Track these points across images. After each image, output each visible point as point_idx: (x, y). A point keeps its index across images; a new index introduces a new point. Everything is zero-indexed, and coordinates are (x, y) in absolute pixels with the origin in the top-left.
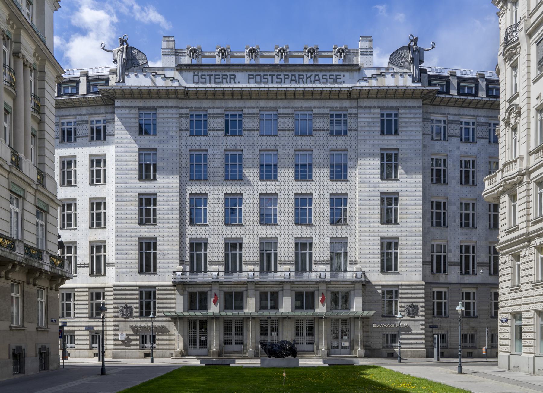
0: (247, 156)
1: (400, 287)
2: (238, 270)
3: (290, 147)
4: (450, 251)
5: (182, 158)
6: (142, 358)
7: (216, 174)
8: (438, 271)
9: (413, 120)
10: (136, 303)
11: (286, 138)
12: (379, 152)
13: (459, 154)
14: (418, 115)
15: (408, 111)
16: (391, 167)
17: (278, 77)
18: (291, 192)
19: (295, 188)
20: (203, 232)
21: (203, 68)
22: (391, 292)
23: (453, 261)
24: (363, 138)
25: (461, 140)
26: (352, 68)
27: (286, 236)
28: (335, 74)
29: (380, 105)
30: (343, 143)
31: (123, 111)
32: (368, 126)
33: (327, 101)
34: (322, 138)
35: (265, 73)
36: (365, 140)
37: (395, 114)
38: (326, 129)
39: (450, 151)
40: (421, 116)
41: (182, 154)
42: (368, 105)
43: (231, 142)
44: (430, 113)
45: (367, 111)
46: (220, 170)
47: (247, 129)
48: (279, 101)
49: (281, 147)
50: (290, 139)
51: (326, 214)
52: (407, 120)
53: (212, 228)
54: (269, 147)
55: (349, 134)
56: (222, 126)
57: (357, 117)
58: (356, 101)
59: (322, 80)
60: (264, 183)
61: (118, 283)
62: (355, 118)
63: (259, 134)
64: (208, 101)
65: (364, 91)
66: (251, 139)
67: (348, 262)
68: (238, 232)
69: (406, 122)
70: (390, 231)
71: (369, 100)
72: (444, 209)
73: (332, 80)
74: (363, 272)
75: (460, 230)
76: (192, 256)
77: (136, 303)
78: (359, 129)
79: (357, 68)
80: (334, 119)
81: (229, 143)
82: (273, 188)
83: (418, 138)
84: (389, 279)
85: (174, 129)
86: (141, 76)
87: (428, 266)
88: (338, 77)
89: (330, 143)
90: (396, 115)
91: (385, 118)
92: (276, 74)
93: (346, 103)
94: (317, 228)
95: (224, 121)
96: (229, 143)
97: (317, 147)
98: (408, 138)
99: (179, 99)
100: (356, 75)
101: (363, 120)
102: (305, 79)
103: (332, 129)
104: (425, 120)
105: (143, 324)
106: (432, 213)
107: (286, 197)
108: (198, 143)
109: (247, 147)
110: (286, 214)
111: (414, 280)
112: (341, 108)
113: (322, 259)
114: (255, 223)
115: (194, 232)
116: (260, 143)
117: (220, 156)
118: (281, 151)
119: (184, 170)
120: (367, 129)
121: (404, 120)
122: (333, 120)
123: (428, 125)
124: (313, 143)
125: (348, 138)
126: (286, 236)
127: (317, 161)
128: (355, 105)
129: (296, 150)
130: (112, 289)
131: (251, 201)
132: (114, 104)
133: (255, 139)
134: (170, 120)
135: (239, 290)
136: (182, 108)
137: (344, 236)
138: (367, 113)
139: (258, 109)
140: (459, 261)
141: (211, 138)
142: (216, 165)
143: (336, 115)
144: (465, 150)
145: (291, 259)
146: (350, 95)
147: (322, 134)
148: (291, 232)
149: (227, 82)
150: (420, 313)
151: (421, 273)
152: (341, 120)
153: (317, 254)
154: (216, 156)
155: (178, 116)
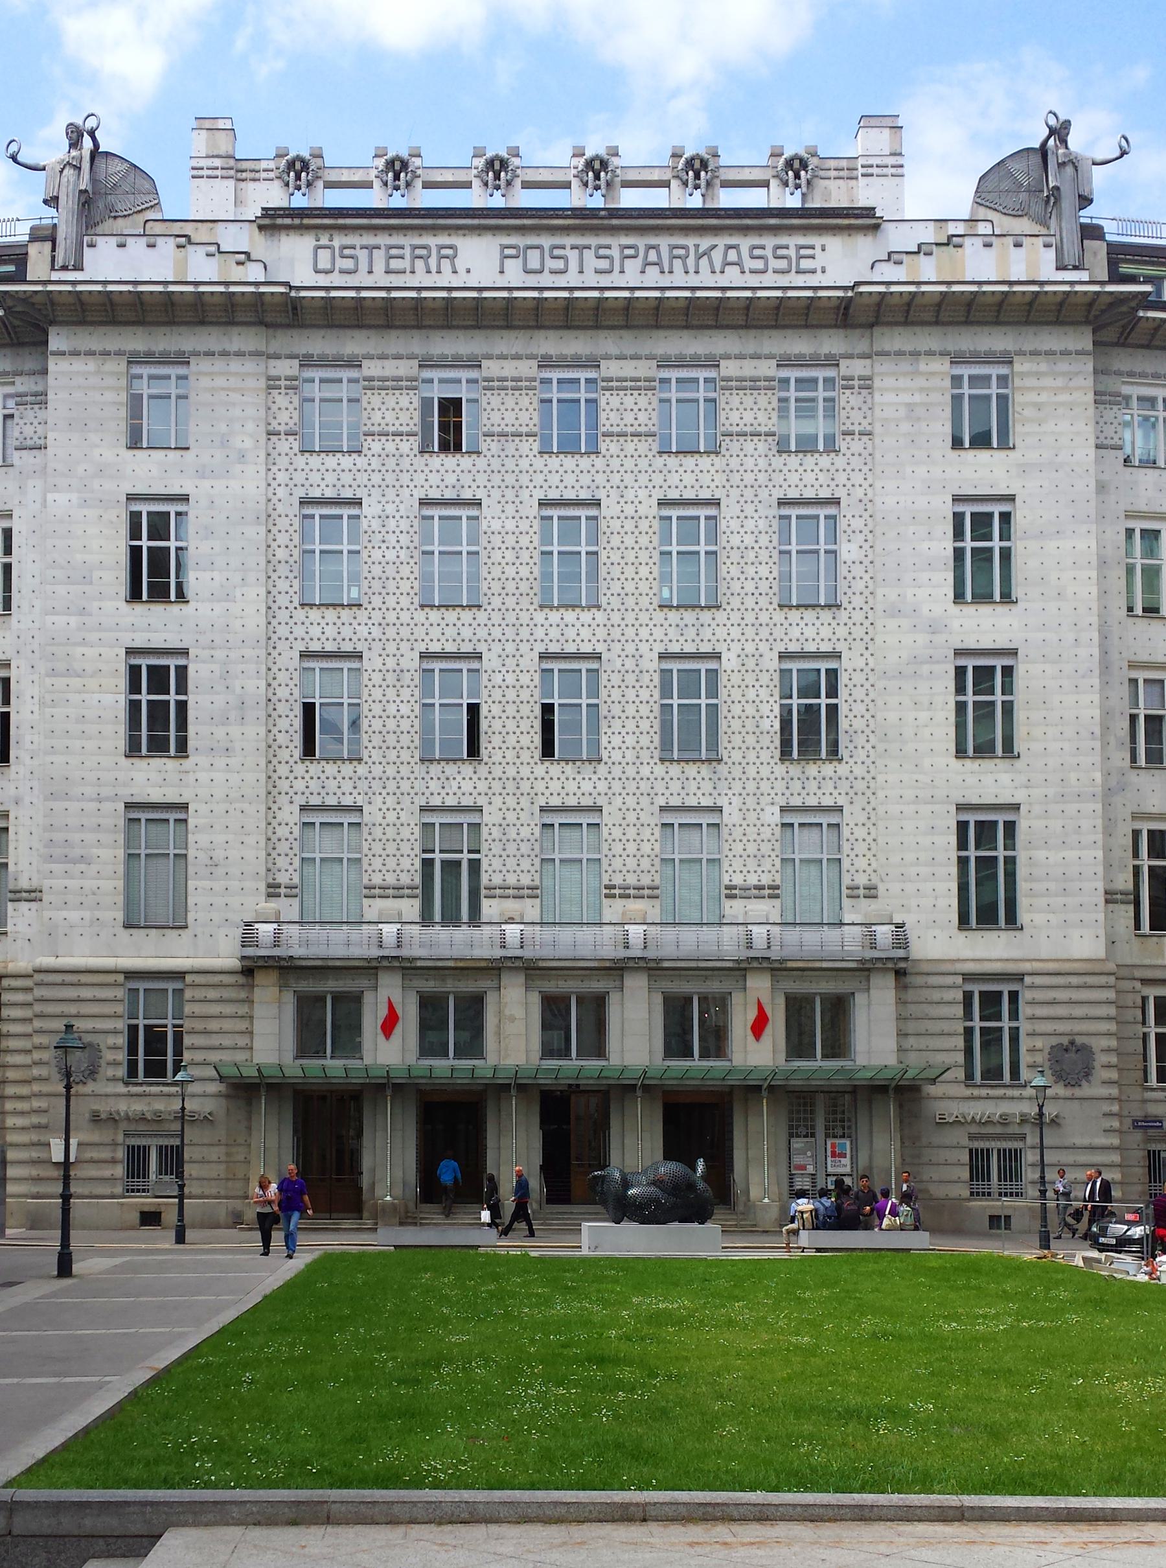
0: (496, 525)
1: (1028, 980)
2: (465, 916)
3: (642, 494)
5: (274, 530)
6: (132, 1228)
7: (391, 586)
9: (1064, 397)
10: (115, 1032)
11: (629, 464)
12: (948, 509)
14: (1079, 381)
15: (1043, 367)
17: (602, 252)
18: (644, 648)
19: (658, 633)
20: (347, 786)
27: (631, 801)
28: (793, 241)
29: (950, 348)
30: (821, 476)
33: (766, 332)
34: (749, 463)
35: (558, 240)
38: (763, 429)
40: (1090, 382)
42: (908, 348)
43: (446, 473)
44: (1119, 373)
45: (905, 365)
46: (405, 571)
47: (496, 429)
48: (603, 334)
49: (613, 492)
50: (643, 463)
51: (765, 724)
53: (377, 770)
54: (570, 495)
55: (842, 444)
56: (410, 419)
58: (868, 333)
59: (749, 264)
60: (554, 616)
61: (48, 961)
63: (536, 447)
64: (365, 332)
65: (896, 300)
66: (510, 464)
68: (467, 786)
69: (1039, 407)
70: (989, 782)
71: (910, 330)
73: (782, 264)
74: (900, 926)
77: (115, 1032)
78: (878, 429)
80: (792, 394)
81: (434, 479)
82: (585, 633)
84: (990, 949)
87: (1123, 907)
88: (803, 252)
89: (778, 478)
90: (1003, 380)
91: (966, 391)
92: (592, 240)
93: (831, 343)
94: (737, 772)
95: (416, 403)
96: (434, 479)
97: (735, 492)
101: (890, 397)
102: (691, 261)
103: (784, 431)
104: (1103, 398)
105: (138, 1107)
107: (630, 664)
108: (330, 478)
110: (631, 725)
111: (1077, 956)
112: (815, 361)
113: (753, 880)
114: (525, 756)
115: (314, 785)
116: (539, 479)
117: (404, 525)
118: (609, 508)
119: (283, 570)
121: (1031, 397)
122: (786, 400)
124: (720, 479)
125: (840, 461)
127: (735, 540)
128: (862, 346)
129: (662, 503)
130: (28, 983)
131: (510, 679)
133: (524, 464)
135: (468, 986)
136: (277, 357)
137: (828, 801)
138: (905, 374)
139: (534, 363)
142: (391, 555)
143: (797, 380)
146: (845, 314)
147: (749, 446)
148: (645, 786)
149: (429, 272)
151: (1102, 933)
152: (813, 400)
153: (737, 864)
154: (392, 524)
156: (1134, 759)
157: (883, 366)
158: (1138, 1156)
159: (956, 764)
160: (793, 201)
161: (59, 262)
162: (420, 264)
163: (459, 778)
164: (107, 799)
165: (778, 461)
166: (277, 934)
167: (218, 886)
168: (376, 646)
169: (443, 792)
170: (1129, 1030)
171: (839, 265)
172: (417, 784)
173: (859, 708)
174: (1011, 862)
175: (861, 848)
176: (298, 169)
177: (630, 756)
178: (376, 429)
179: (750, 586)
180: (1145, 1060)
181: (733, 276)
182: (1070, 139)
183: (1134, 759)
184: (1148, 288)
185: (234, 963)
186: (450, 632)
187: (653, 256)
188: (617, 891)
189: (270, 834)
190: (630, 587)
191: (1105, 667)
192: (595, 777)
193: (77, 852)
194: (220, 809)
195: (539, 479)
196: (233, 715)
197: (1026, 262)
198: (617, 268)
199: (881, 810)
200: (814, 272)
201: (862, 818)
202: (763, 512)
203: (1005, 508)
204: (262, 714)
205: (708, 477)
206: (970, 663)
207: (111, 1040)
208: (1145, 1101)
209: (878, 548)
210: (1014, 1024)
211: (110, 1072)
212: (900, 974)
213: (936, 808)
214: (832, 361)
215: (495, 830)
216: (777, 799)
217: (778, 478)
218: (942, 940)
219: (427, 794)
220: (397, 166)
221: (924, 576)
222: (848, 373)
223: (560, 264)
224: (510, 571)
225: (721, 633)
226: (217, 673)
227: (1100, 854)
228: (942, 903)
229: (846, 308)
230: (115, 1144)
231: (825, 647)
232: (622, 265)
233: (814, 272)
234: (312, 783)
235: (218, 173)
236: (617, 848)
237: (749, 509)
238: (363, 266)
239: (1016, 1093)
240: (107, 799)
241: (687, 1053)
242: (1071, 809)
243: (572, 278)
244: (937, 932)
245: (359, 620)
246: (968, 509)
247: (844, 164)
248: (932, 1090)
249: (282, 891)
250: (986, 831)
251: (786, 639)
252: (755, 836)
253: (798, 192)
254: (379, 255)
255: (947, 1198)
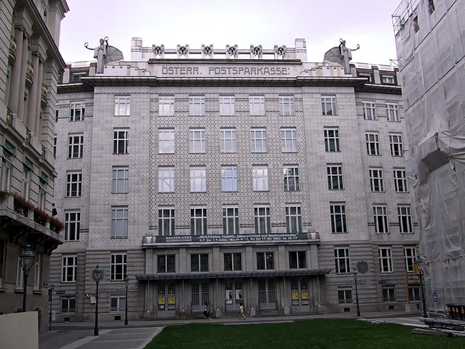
0: (209, 133)
1: (350, 246)
4: (390, 213)
5: (152, 135)
6: (113, 321)
7: (182, 149)
8: (381, 230)
9: (348, 103)
10: (108, 267)
13: (388, 131)
14: (352, 100)
16: (334, 141)
17: (234, 69)
18: (248, 163)
20: (171, 200)
21: (171, 62)
22: (341, 251)
23: (393, 221)
24: (308, 117)
25: (388, 119)
26: (295, 63)
27: (246, 202)
29: (321, 92)
31: (102, 96)
32: (311, 108)
34: (273, 118)
36: (310, 120)
37: (333, 99)
38: (276, 110)
39: (381, 128)
41: (152, 132)
42: (311, 92)
44: (361, 98)
45: (310, 95)
48: (235, 88)
51: (280, 182)
52: (344, 103)
53: (179, 195)
57: (302, 101)
58: (300, 88)
59: (271, 72)
62: (301, 102)
66: (212, 119)
67: (302, 224)
68: (203, 199)
69: (343, 106)
70: (338, 196)
72: (381, 176)
73: (279, 72)
74: (318, 233)
75: (396, 194)
76: (160, 221)
77: (108, 267)
78: (304, 110)
79: (298, 63)
83: (353, 117)
85: (146, 111)
86: (117, 68)
87: (372, 227)
88: (284, 69)
89: (280, 122)
91: (325, 101)
93: (292, 90)
94: (273, 194)
96: (193, 122)
97: (270, 125)
98: (346, 117)
99: (150, 86)
100: (298, 68)
102: (256, 72)
104: (357, 104)
106: (371, 180)
107: (245, 167)
108: (166, 122)
109: (209, 126)
110: (245, 183)
113: (279, 222)
115: (162, 200)
120: (311, 110)
123: (361, 107)
124: (266, 122)
126: (245, 202)
127: (270, 137)
132: (93, 91)
134: (142, 103)
137: (297, 201)
139: (218, 95)
140: (398, 222)
141: (178, 119)
142: (182, 141)
144: (393, 128)
145: (251, 223)
147: (273, 114)
150: (370, 270)
153: (275, 218)
154: (182, 133)
155: (149, 100)
156: (372, 190)
157: (304, 96)
158: (380, 291)
159: (329, 192)
160: (281, 58)
161: (98, 71)
162: (189, 72)
163: (200, 197)
164: (106, 205)
165: (280, 118)
166: (152, 239)
167: (135, 227)
168: (178, 164)
169: (196, 201)
170: (376, 258)
171: (292, 73)
172: (189, 199)
173: (305, 178)
174: (344, 216)
175: (306, 213)
176: (158, 50)
177: (245, 191)
178: (178, 110)
179: (275, 148)
180: (380, 266)
181: (267, 75)
182: (346, 45)
183: (372, 190)
184: (367, 79)
185: (141, 248)
186: (197, 160)
187: (247, 70)
188: (243, 226)
189: (150, 212)
190: (244, 148)
191: (363, 168)
192: (236, 196)
193: (98, 219)
194: (136, 207)
195: (220, 122)
196: (140, 182)
197: (338, 72)
198: (238, 73)
199: (311, 203)
200: (287, 74)
201: (306, 205)
202: (277, 130)
203: (337, 129)
204: (148, 182)
205: (263, 122)
206: (331, 166)
207: (107, 269)
208: (381, 276)
209: (306, 139)
210: (348, 257)
211: (107, 278)
212: (318, 245)
213: (325, 202)
214: (292, 95)
215: (210, 210)
216: (284, 201)
217: (280, 122)
218: (328, 236)
219: (192, 201)
220: (183, 49)
221: (318, 146)
222: (296, 98)
223: (224, 72)
224: (213, 145)
225: (268, 159)
226: (136, 171)
227: (366, 214)
228: (328, 227)
229: (295, 82)
230: (108, 298)
231: (294, 163)
232: (239, 72)
233: (287, 74)
234: (162, 200)
235: (138, 50)
236: (243, 214)
237: (274, 129)
238: (175, 72)
239: (349, 276)
240: (106, 205)
241: (263, 268)
242: (358, 203)
243: (227, 75)
244: (326, 234)
245: (174, 157)
246: (328, 129)
247: (292, 49)
248: (327, 275)
249: (153, 228)
250: (337, 209)
251: (284, 161)
252: (279, 211)
253: (282, 56)
254: (179, 70)
255: (333, 304)
